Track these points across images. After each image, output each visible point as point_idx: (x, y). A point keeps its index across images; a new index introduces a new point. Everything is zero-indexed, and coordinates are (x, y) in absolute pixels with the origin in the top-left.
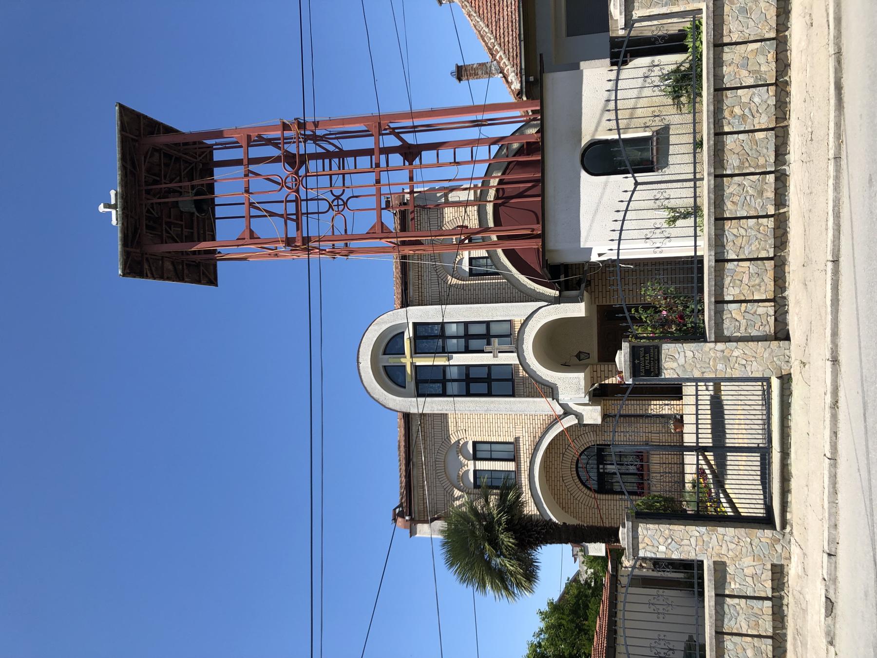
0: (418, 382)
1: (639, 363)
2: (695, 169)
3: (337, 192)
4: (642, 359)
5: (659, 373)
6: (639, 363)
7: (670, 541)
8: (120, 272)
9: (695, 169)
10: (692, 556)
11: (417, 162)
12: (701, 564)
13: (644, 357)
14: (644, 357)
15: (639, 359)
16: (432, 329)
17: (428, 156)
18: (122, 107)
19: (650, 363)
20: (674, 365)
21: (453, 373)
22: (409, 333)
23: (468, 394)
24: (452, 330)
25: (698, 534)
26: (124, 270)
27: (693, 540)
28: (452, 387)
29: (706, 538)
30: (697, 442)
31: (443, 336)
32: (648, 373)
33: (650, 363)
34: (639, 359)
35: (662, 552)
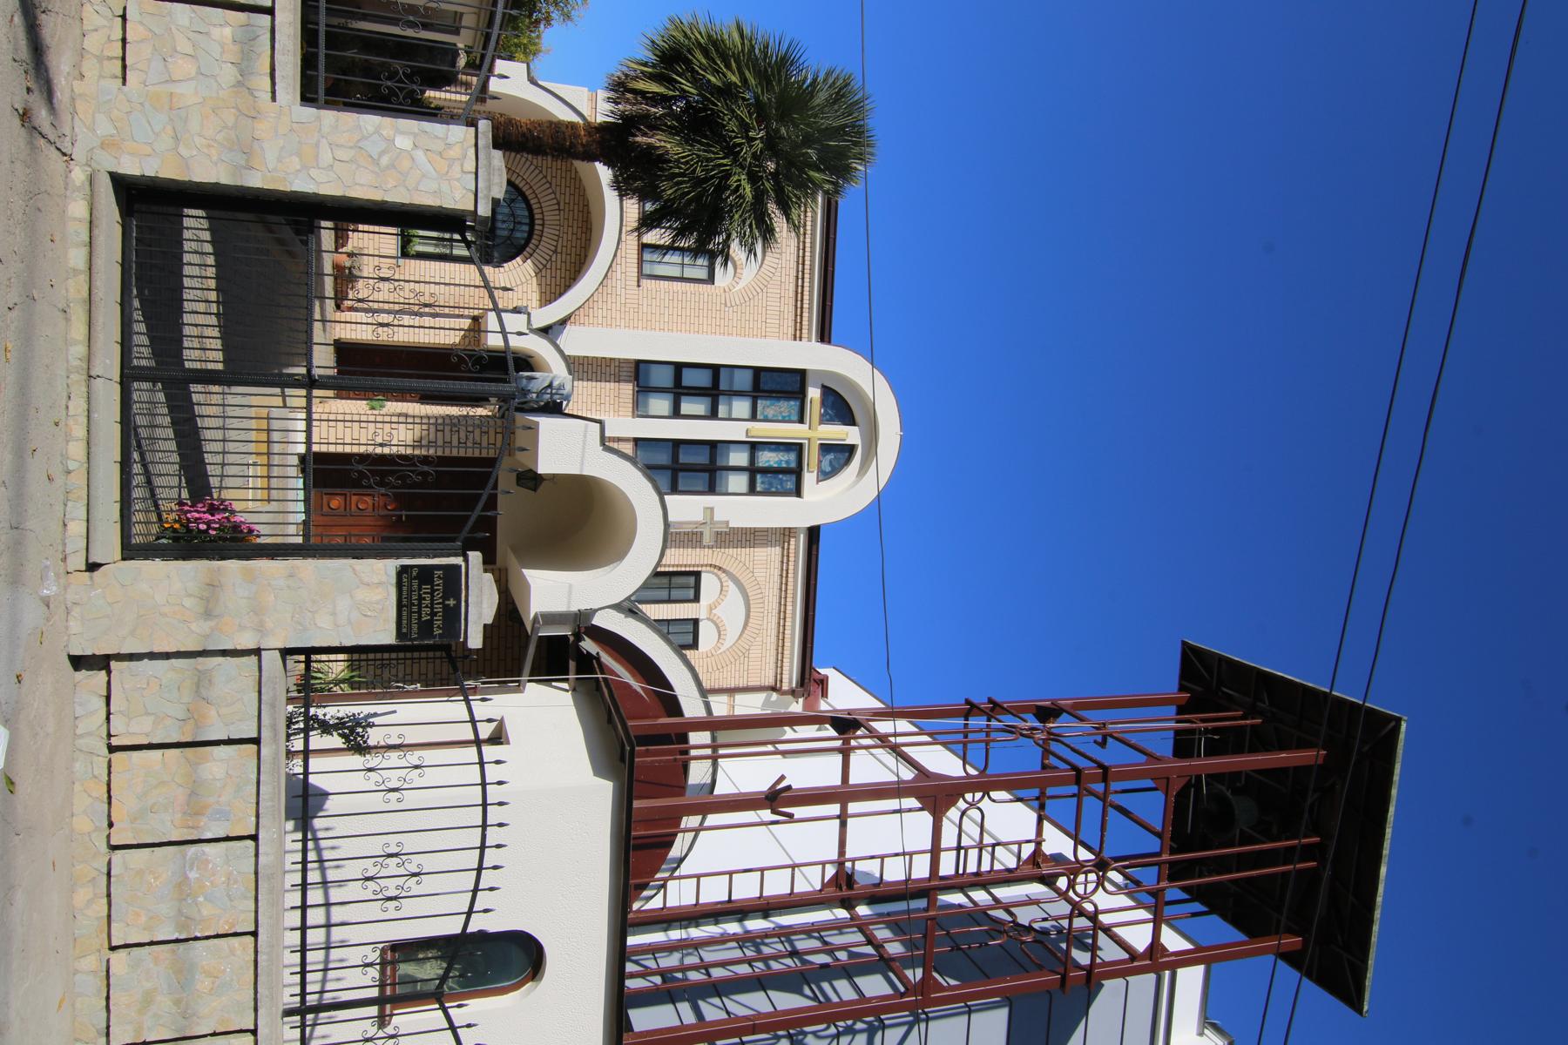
0: (800, 394)
1: (445, 598)
2: (304, 878)
3: (974, 813)
4: (438, 608)
5: (403, 571)
6: (445, 598)
7: (385, 161)
8: (1404, 726)
9: (304, 878)
10: (329, 117)
11: (831, 871)
12: (308, 97)
13: (433, 614)
14: (433, 614)
15: (446, 607)
16: (771, 484)
17: (811, 881)
18: (1359, 1010)
19: (420, 599)
20: (362, 594)
21: (741, 407)
22: (809, 478)
23: (715, 369)
24: (738, 482)
25: (313, 172)
26: (1396, 730)
27: (326, 156)
28: (744, 381)
29: (295, 163)
30: (309, 398)
31: (753, 471)
32: (426, 574)
33: (420, 599)
34: (446, 607)
35: (402, 133)
